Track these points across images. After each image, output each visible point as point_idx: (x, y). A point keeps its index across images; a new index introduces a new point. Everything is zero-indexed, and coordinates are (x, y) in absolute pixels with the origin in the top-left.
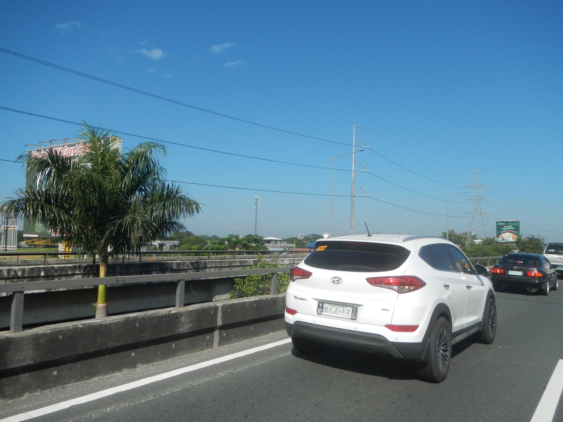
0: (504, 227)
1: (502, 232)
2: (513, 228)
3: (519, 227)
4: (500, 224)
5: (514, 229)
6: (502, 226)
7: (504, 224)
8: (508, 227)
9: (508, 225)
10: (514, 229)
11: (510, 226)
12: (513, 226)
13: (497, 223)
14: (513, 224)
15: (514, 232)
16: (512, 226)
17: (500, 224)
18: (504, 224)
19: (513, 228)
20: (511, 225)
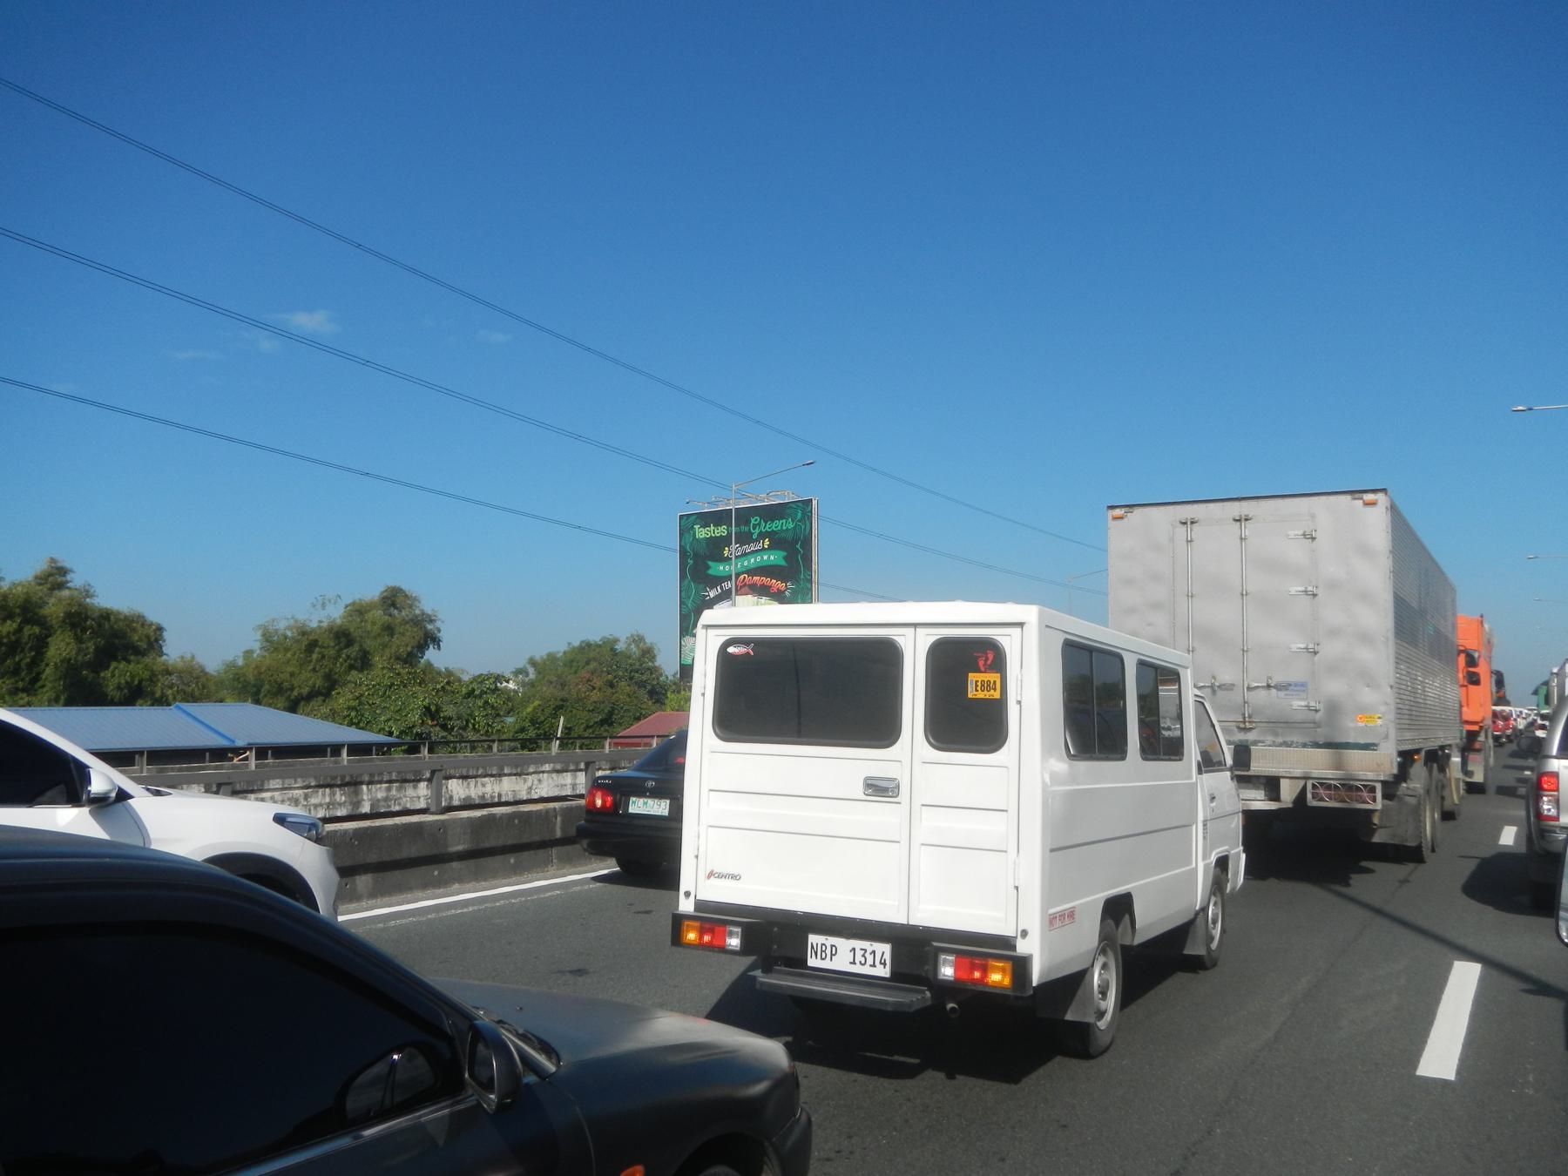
0: (726, 553)
1: (712, 594)
2: (775, 558)
3: (807, 542)
4: (702, 533)
5: (782, 563)
6: (715, 549)
7: (721, 531)
8: (745, 555)
9: (744, 539)
10: (782, 563)
11: (757, 540)
12: (777, 542)
13: (687, 523)
14: (777, 525)
15: (782, 585)
16: (767, 542)
17: (702, 533)
18: (721, 531)
19: (775, 558)
20: (762, 536)
